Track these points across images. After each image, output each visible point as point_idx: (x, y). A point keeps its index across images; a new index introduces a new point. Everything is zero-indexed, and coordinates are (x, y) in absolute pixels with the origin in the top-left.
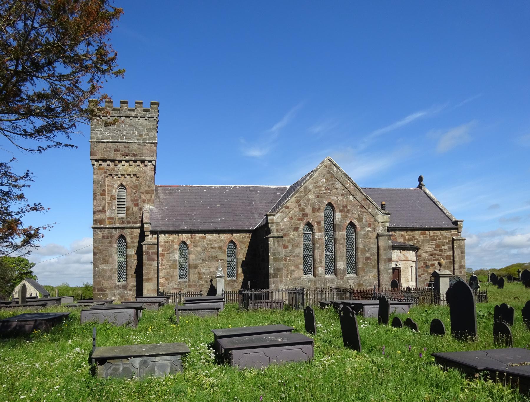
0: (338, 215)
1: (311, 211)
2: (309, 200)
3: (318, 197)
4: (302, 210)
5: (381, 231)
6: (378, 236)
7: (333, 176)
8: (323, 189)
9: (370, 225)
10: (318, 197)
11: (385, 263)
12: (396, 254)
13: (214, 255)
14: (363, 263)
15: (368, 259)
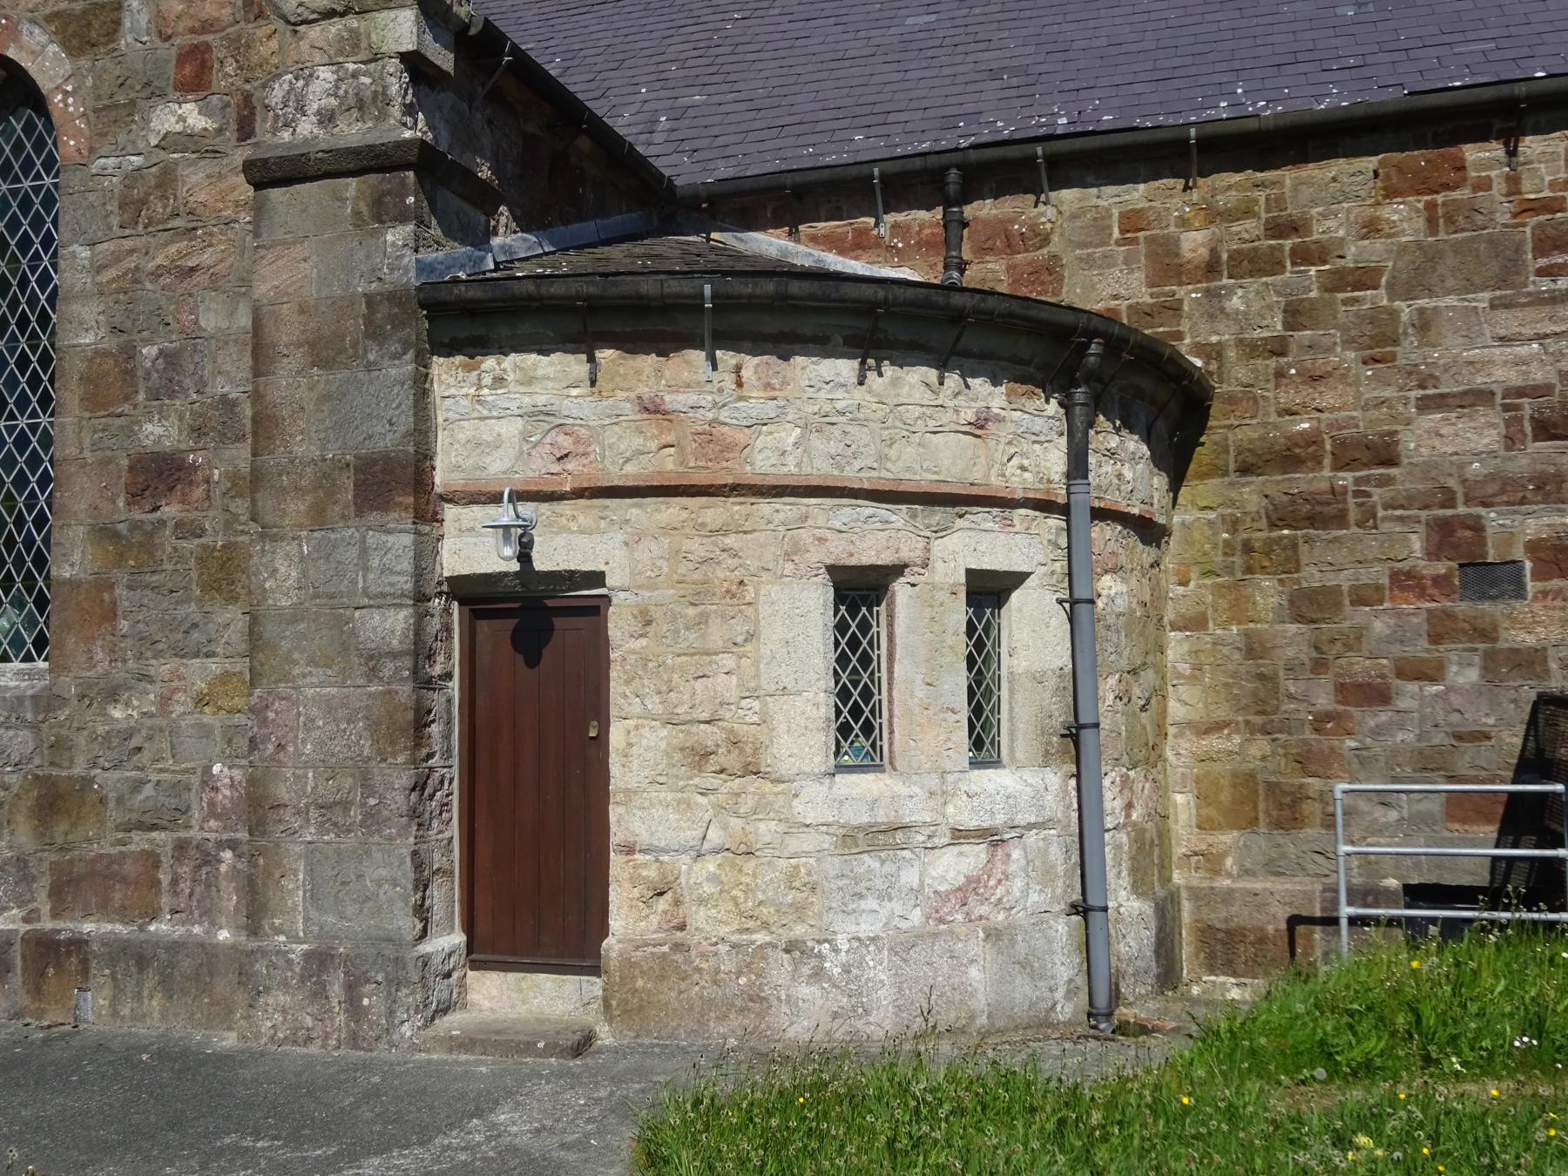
5: (327, 118)
9: (194, 74)
11: (319, 518)
12: (499, 414)
14: (104, 533)
15: (159, 475)
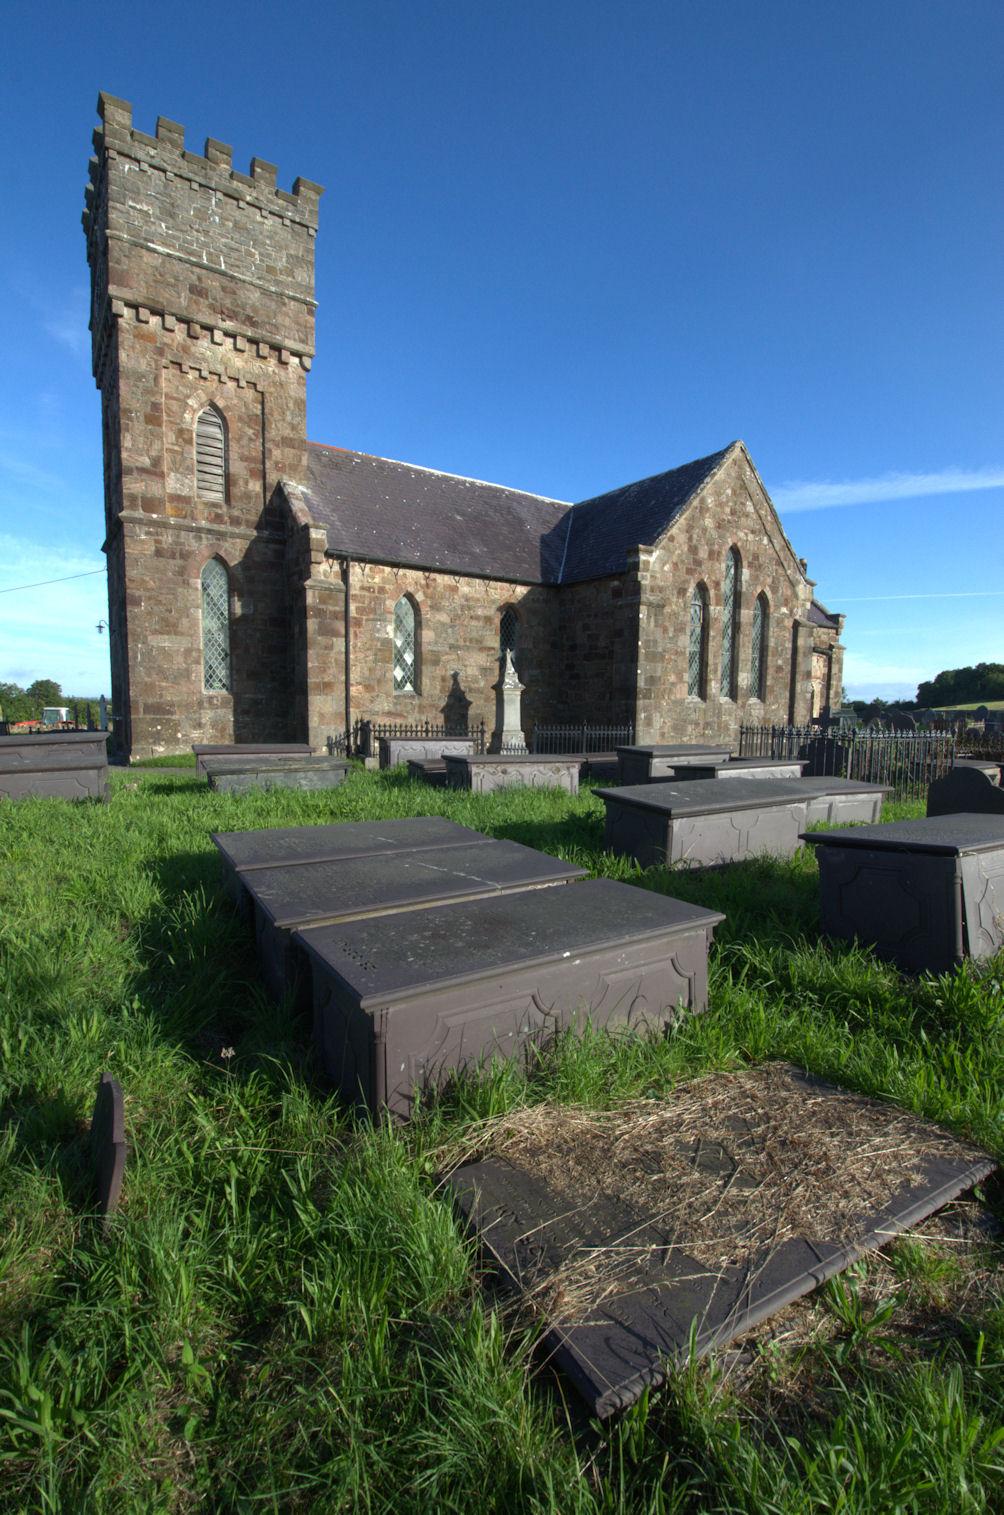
0: (746, 573)
1: (706, 556)
2: (705, 530)
3: (719, 527)
4: (693, 550)
6: (796, 625)
7: (744, 487)
8: (728, 510)
10: (719, 527)
13: (474, 635)
